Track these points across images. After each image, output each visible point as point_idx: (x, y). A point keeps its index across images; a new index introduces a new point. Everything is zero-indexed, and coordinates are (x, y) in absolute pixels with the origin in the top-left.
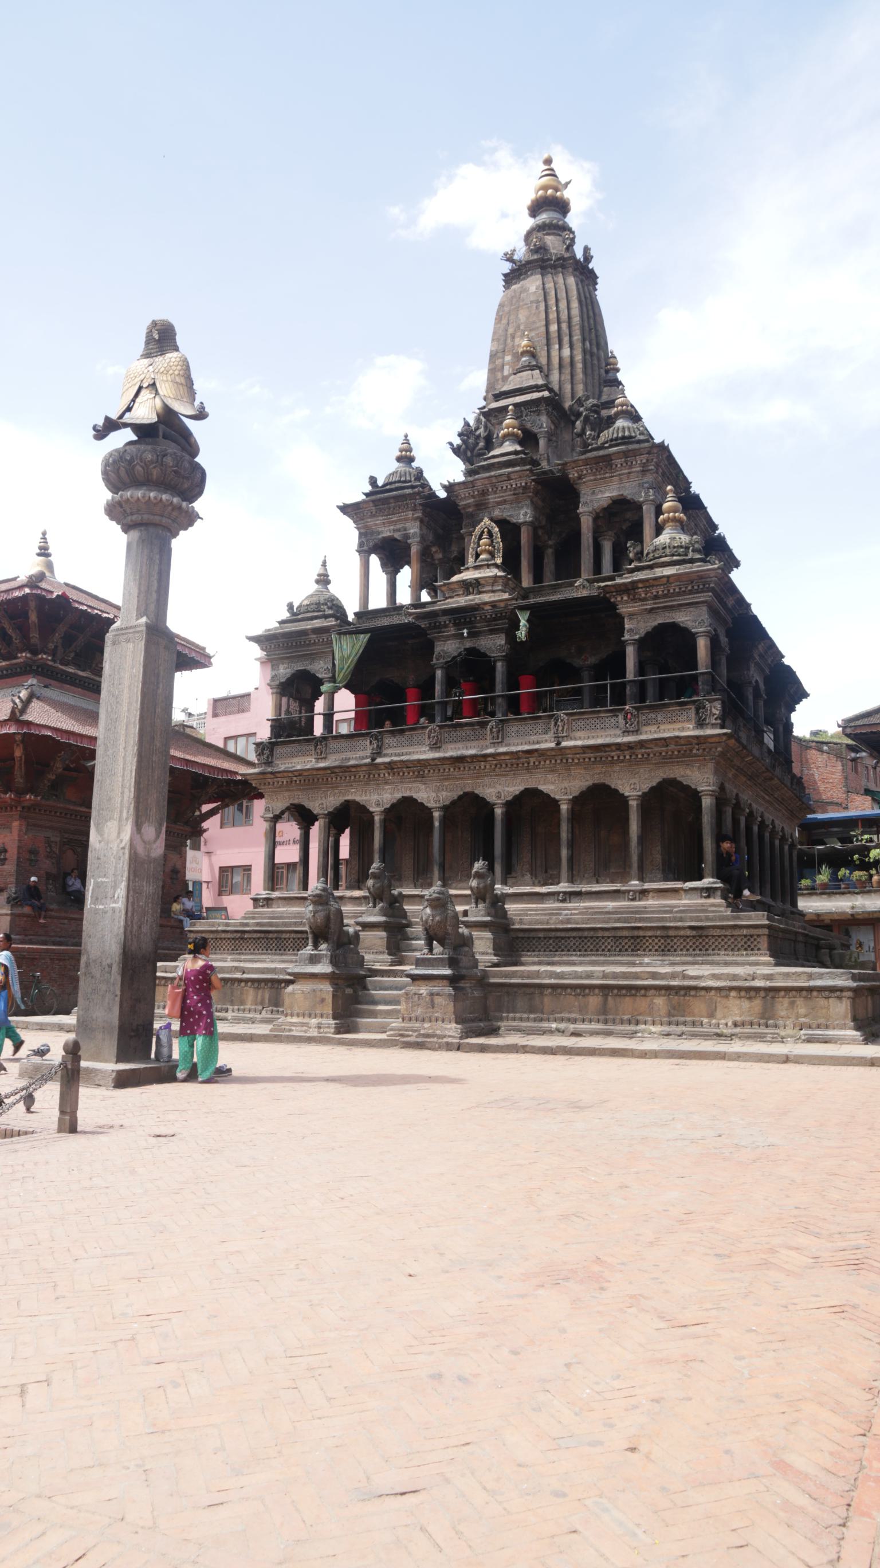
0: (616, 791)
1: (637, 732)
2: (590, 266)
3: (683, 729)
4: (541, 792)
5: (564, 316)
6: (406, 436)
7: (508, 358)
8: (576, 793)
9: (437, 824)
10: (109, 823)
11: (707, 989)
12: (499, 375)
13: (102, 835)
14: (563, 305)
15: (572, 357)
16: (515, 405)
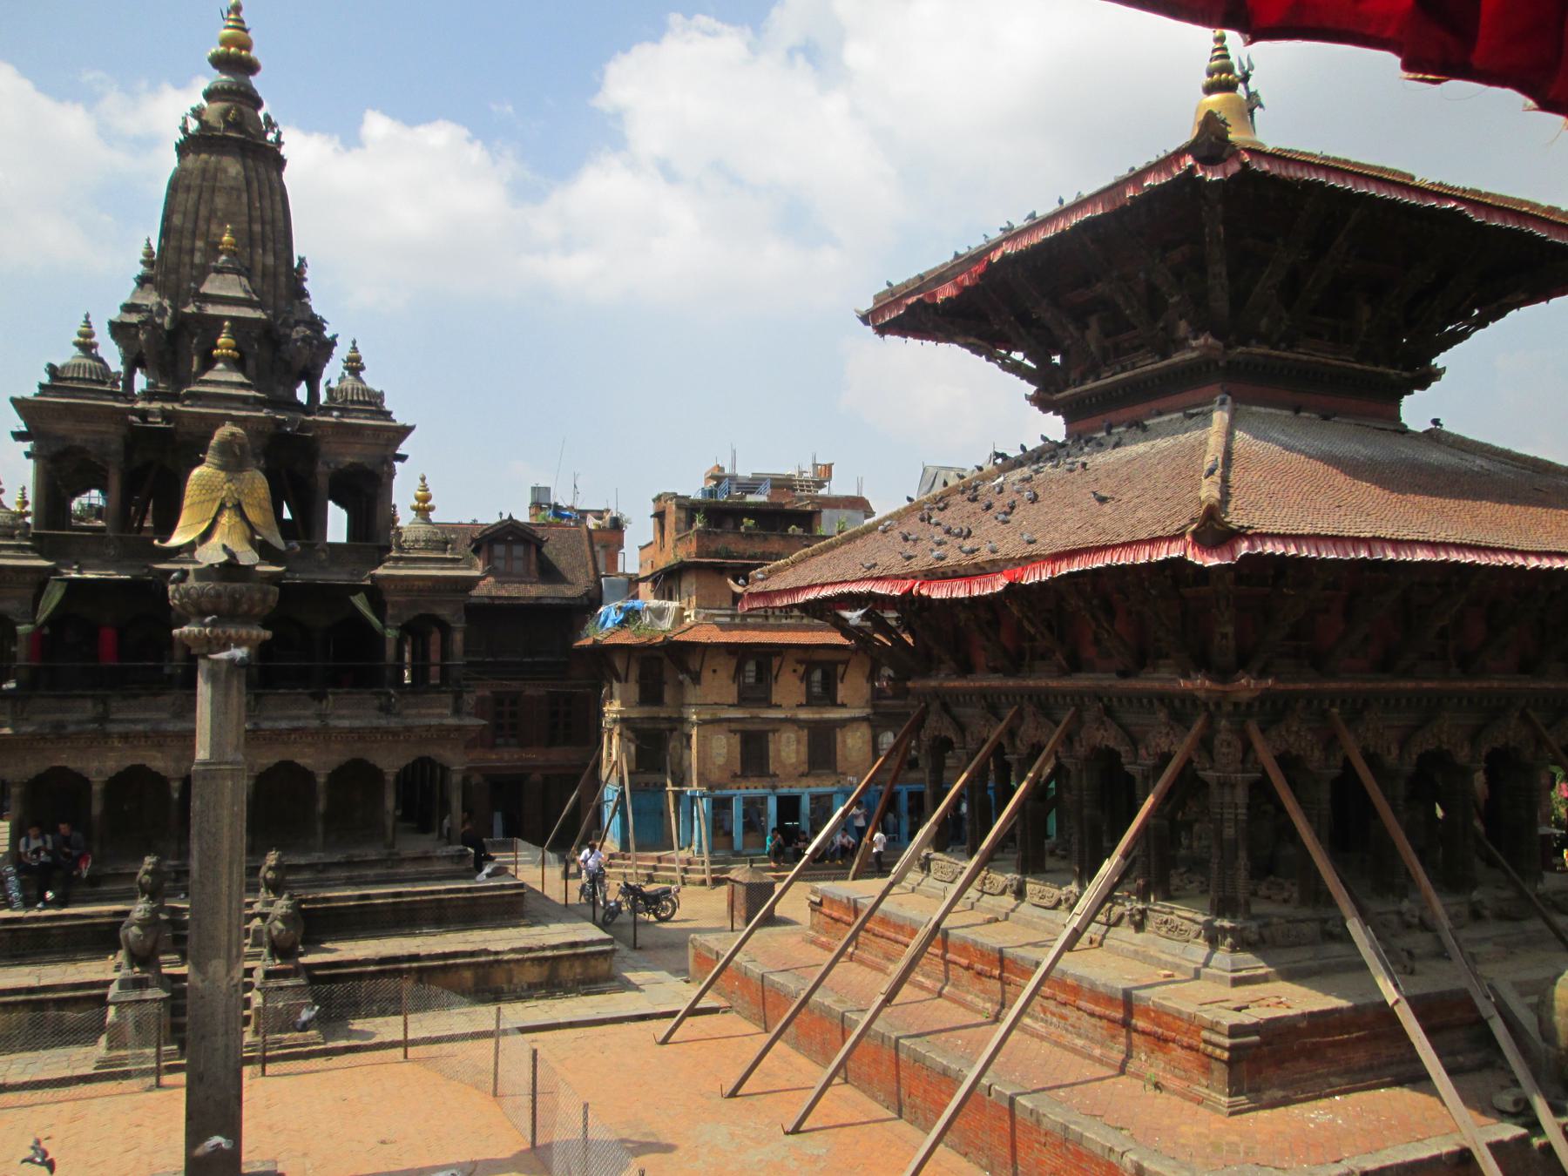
0: (374, 767)
1: (398, 715)
2: (283, 151)
3: (441, 716)
4: (297, 765)
5: (268, 213)
6: (87, 316)
7: (199, 244)
8: (335, 767)
9: (176, 795)
10: (214, 963)
11: (508, 962)
12: (186, 259)
13: (205, 973)
14: (267, 203)
15: (275, 267)
16: (232, 319)
